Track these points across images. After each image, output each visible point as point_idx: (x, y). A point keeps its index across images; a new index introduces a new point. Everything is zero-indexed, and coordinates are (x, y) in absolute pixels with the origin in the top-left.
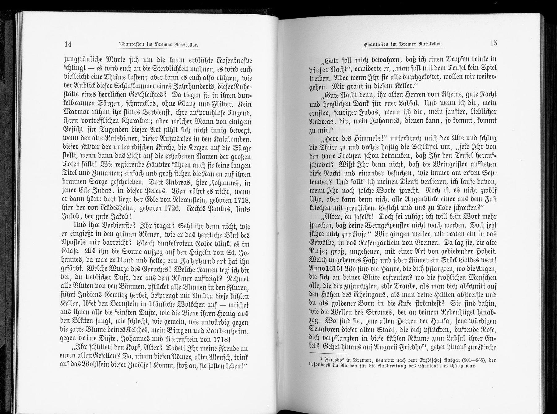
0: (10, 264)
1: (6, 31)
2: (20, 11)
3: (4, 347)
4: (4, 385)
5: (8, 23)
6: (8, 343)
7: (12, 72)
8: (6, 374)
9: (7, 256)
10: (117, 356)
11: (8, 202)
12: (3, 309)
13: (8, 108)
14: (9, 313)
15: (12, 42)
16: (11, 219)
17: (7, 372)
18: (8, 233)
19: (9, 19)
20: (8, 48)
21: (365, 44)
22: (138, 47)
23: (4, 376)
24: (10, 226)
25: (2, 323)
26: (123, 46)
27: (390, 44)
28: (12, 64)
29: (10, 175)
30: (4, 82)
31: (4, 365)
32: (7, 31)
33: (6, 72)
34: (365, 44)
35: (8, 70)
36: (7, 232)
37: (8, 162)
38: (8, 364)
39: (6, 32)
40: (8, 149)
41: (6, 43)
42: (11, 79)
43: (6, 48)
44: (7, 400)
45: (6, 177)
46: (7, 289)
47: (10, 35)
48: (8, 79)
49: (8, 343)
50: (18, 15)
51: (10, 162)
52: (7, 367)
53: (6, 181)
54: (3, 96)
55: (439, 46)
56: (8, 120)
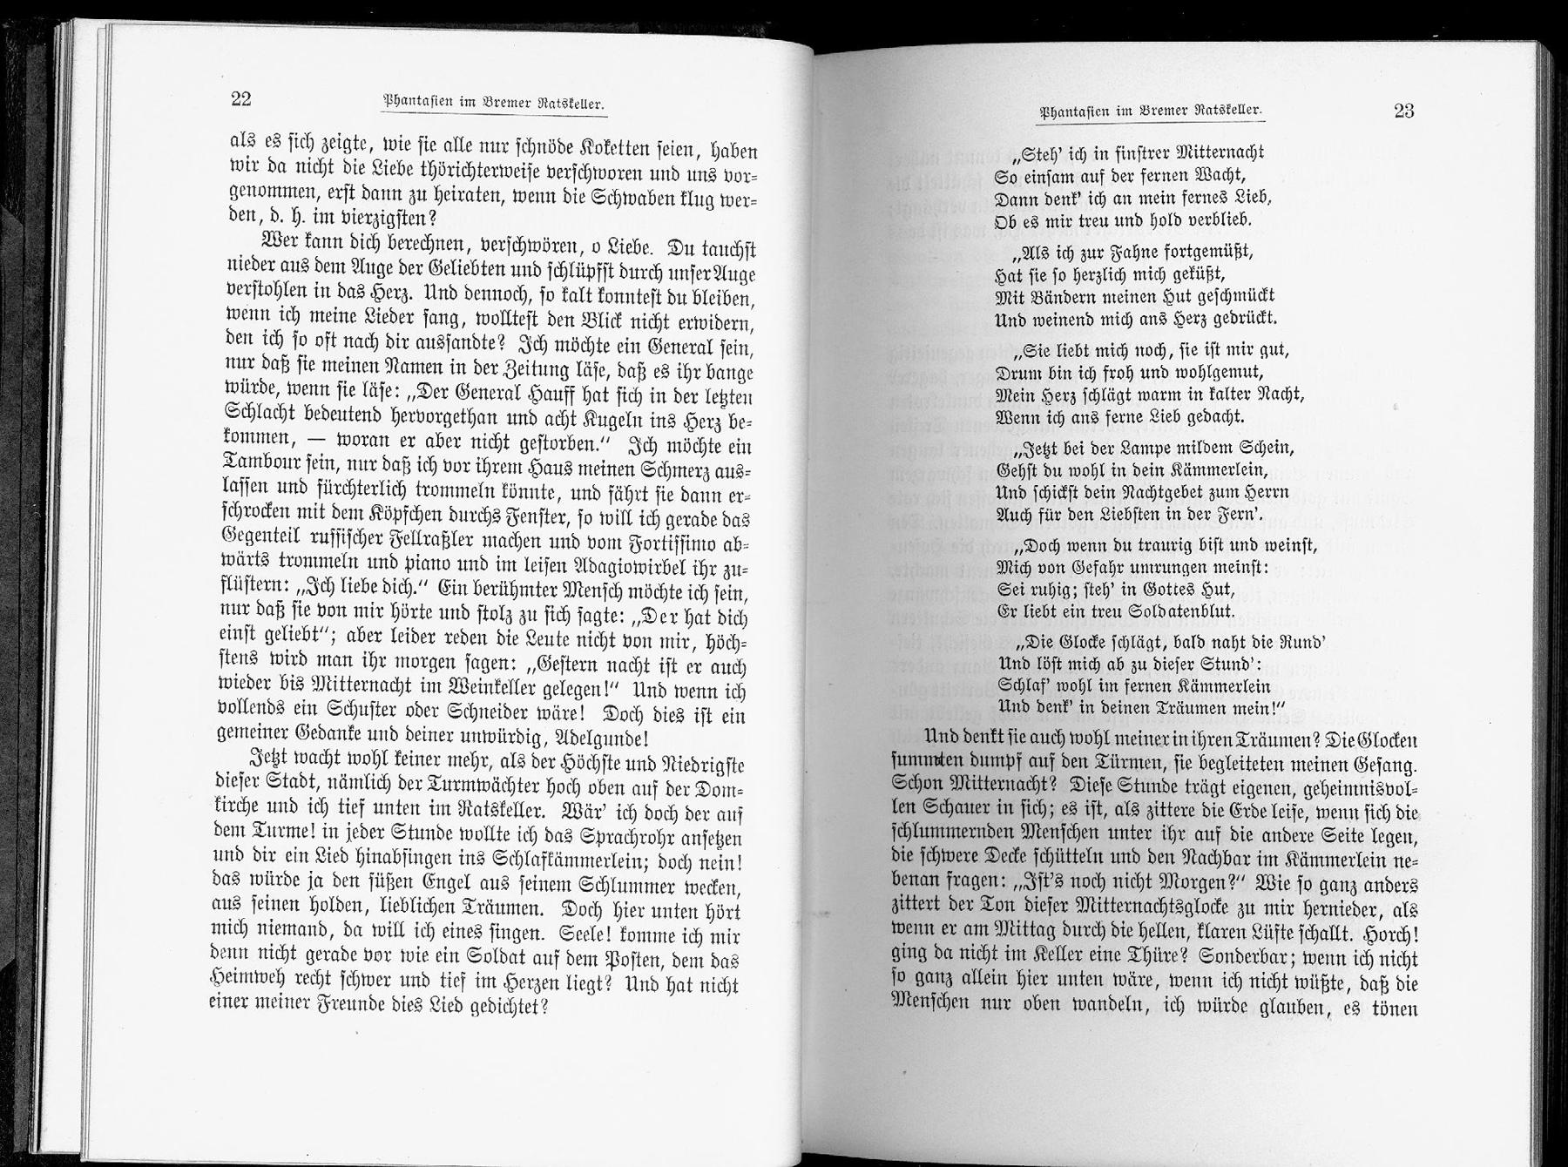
0: (34, 732)
1: (29, 75)
2: (67, 17)
3: (12, 967)
4: (11, 1074)
5: (35, 54)
6: (22, 955)
7: (43, 191)
8: (18, 1043)
9: (23, 710)
11: (27, 558)
12: (10, 860)
13: (32, 292)
14: (27, 869)
15: (44, 107)
16: (36, 606)
17: (19, 1037)
18: (28, 643)
19: (40, 43)
20: (33, 122)
21: (1044, 113)
22: (1092, 120)
23: (11, 1049)
24: (33, 624)
25: (8, 898)
26: (1049, 120)
27: (1113, 112)
28: (43, 169)
29: (36, 482)
30: (22, 220)
31: (13, 1020)
32: (33, 78)
33: (28, 192)
34: (1044, 113)
38: (21, 1016)
39: (29, 79)
40: (29, 407)
41: (29, 110)
42: (41, 212)
43: (28, 123)
44: (18, 1119)
45: (25, 486)
46: (22, 802)
47: (39, 88)
48: (33, 212)
49: (22, 955)
50: (61, 30)
51: (36, 444)
52: (19, 1023)
53: (24, 497)
56: (32, 326)
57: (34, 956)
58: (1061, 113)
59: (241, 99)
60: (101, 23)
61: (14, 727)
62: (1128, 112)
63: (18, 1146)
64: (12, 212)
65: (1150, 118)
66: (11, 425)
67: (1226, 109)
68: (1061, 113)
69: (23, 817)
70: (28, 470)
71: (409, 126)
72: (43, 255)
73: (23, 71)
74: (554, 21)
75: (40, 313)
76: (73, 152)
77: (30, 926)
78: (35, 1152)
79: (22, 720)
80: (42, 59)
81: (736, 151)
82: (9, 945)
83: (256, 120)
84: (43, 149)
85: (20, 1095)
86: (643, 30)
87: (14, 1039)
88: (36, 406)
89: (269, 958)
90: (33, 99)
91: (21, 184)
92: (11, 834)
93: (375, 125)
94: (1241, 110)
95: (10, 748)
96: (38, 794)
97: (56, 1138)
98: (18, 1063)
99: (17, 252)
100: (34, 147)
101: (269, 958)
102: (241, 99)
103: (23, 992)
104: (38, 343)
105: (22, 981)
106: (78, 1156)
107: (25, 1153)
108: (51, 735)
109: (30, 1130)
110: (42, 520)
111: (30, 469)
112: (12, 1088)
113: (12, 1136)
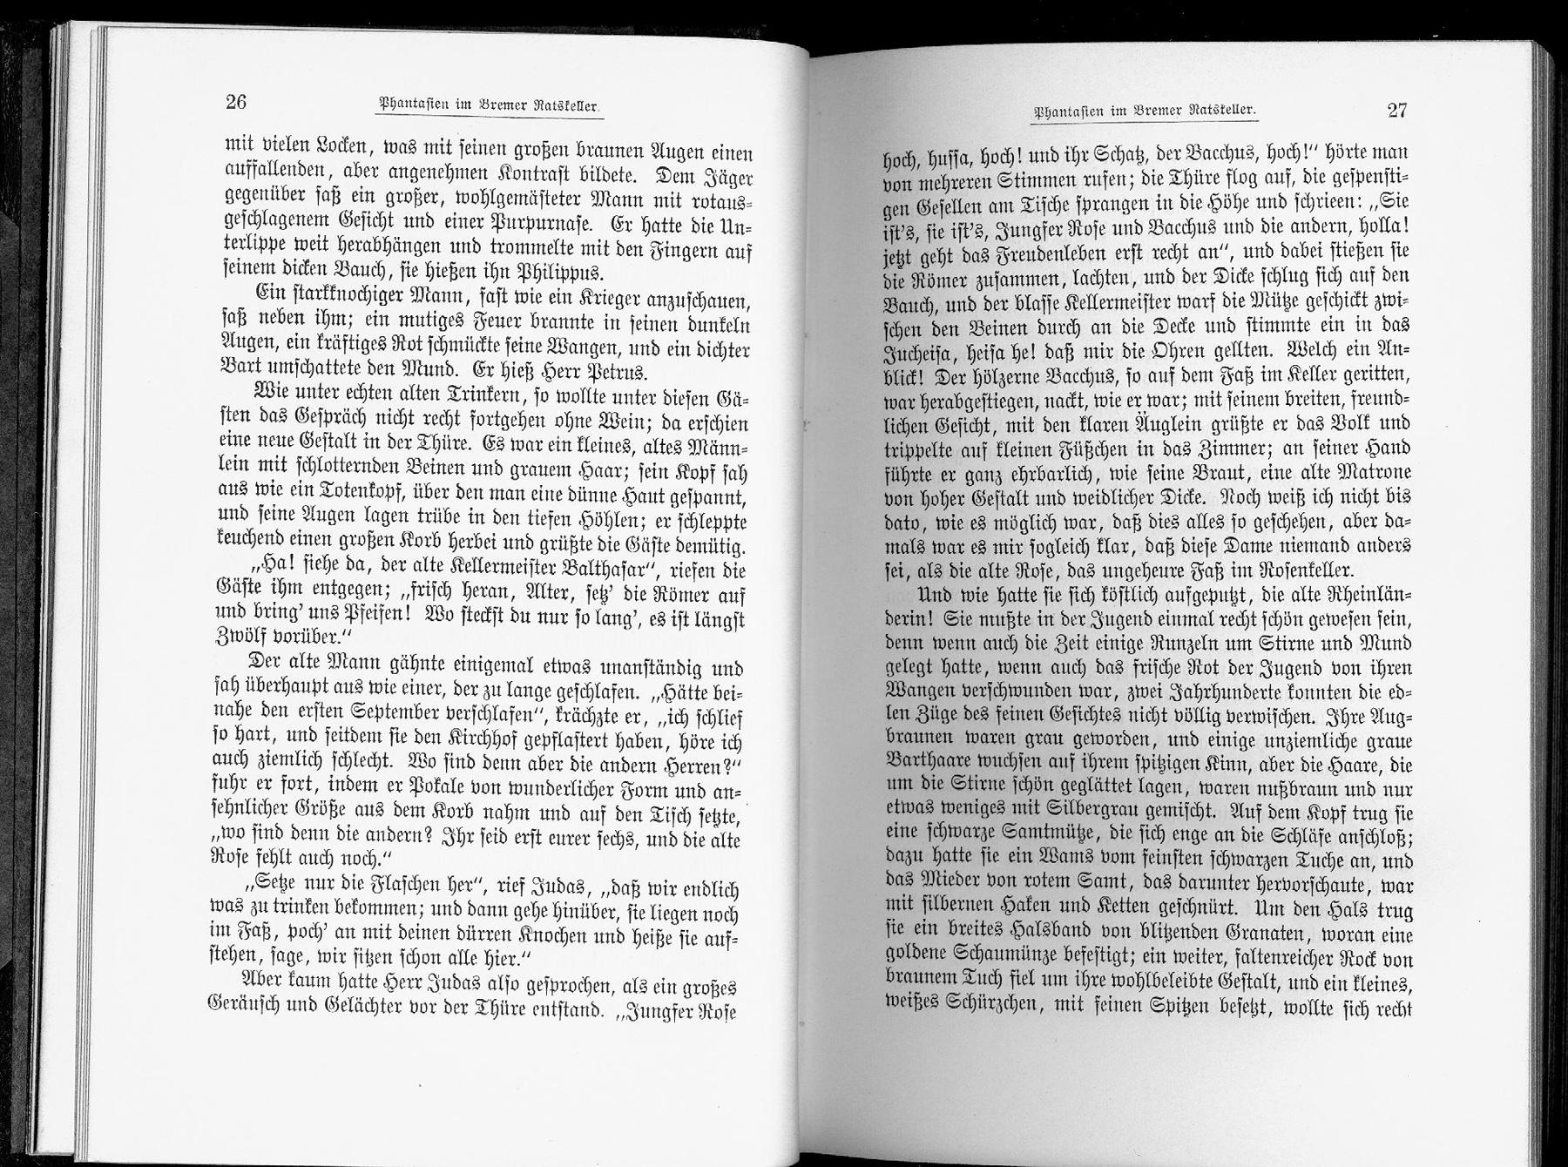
0: (30, 734)
2: (64, 18)
4: (8, 1076)
5: (31, 56)
6: (19, 957)
7: (39, 192)
9: (20, 712)
10: (424, 837)
11: (23, 560)
12: (7, 861)
13: (28, 295)
14: (24, 871)
15: (40, 109)
17: (15, 1038)
19: (35, 46)
20: (28, 125)
23: (8, 1050)
25: (5, 900)
28: (39, 171)
29: (32, 483)
30: (18, 223)
32: (28, 80)
33: (24, 195)
35: (28, 189)
36: (20, 644)
37: (25, 447)
38: (18, 1017)
39: (25, 82)
41: (25, 113)
42: (37, 213)
43: (23, 126)
44: (15, 1120)
45: (21, 487)
46: (19, 804)
49: (19, 957)
50: (57, 32)
51: (32, 447)
52: (16, 1024)
53: (20, 500)
54: (15, 262)
55: (1246, 117)
56: (28, 328)
57: (31, 957)
58: (1055, 113)
59: (236, 102)
60: (94, 25)
61: (11, 728)
62: (1123, 111)
63: (15, 1148)
64: (8, 214)
65: (1144, 117)
66: (8, 427)
67: (1222, 109)
68: (1055, 113)
69: (20, 819)
70: (24, 471)
71: (401, 128)
72: (38, 256)
73: (18, 75)
74: (550, 25)
75: (36, 315)
76: (70, 154)
77: (27, 927)
78: (31, 1153)
79: (19, 722)
80: (38, 62)
81: (733, 154)
82: (6, 947)
83: (255, 123)
84: (39, 152)
85: (16, 1097)
86: (638, 32)
87: (10, 1040)
88: (32, 408)
89: (257, 966)
90: (28, 102)
91: (16, 186)
92: (8, 836)
93: (376, 129)
94: (1236, 110)
95: (6, 749)
96: (34, 795)
97: (53, 1139)
98: (15, 1063)
99: (13, 254)
100: (29, 149)
101: (257, 966)
102: (236, 102)
103: (20, 994)
104: (35, 345)
105: (19, 981)
106: (72, 1157)
107: (23, 1155)
108: (48, 737)
109: (27, 1132)
110: (38, 521)
111: (27, 472)
112: (9, 1089)
113: (9, 1137)
